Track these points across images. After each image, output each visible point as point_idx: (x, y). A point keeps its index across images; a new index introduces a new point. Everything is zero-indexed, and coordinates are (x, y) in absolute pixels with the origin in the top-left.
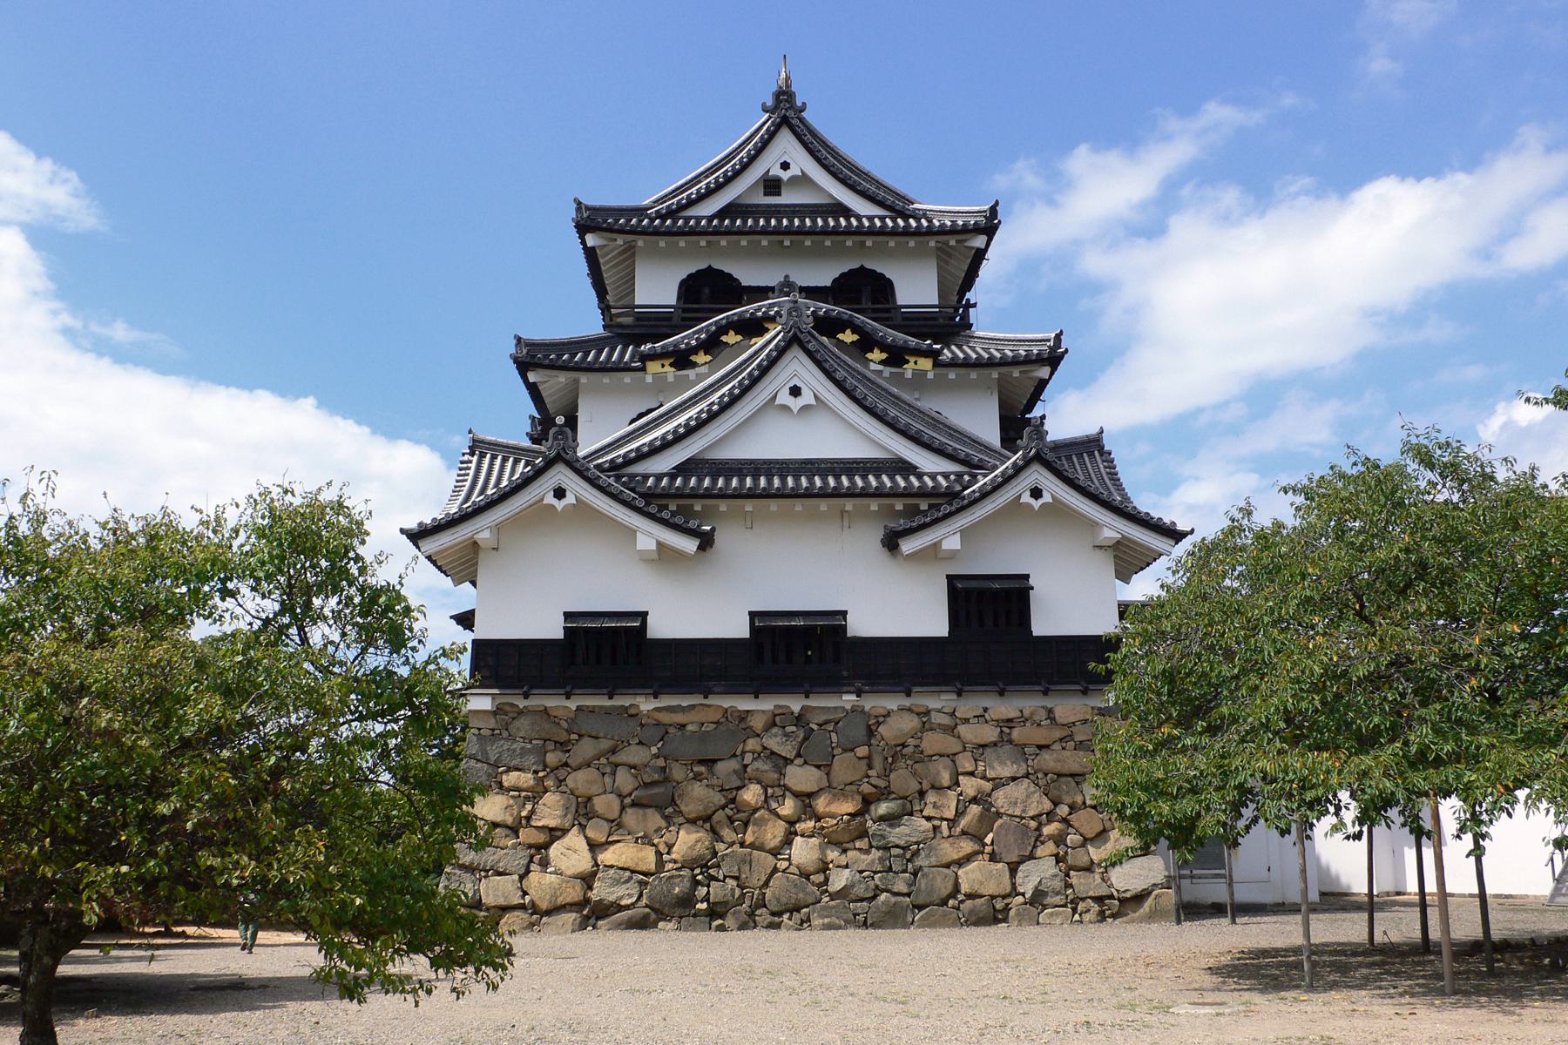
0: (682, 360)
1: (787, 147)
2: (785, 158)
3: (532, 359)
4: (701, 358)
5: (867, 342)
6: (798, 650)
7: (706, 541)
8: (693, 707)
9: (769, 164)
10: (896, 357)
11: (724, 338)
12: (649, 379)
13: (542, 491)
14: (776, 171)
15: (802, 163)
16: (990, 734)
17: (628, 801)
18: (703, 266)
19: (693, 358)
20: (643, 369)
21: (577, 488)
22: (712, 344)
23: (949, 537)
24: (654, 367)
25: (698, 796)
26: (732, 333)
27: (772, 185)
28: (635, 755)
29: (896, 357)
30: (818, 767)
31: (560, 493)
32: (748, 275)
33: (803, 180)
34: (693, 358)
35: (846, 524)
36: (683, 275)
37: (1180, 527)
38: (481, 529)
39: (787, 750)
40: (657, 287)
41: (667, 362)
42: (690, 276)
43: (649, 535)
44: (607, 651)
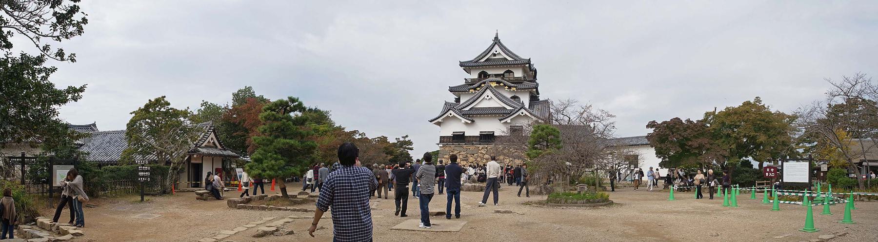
0: (475, 89)
1: (497, 48)
3: (452, 90)
5: (505, 85)
6: (487, 138)
7: (473, 121)
9: (493, 51)
10: (510, 87)
13: (448, 114)
15: (499, 50)
21: (453, 113)
22: (479, 86)
23: (508, 120)
25: (471, 159)
27: (495, 55)
29: (510, 87)
32: (489, 72)
33: (499, 54)
38: (440, 120)
40: (475, 75)
43: (464, 120)
44: (459, 138)
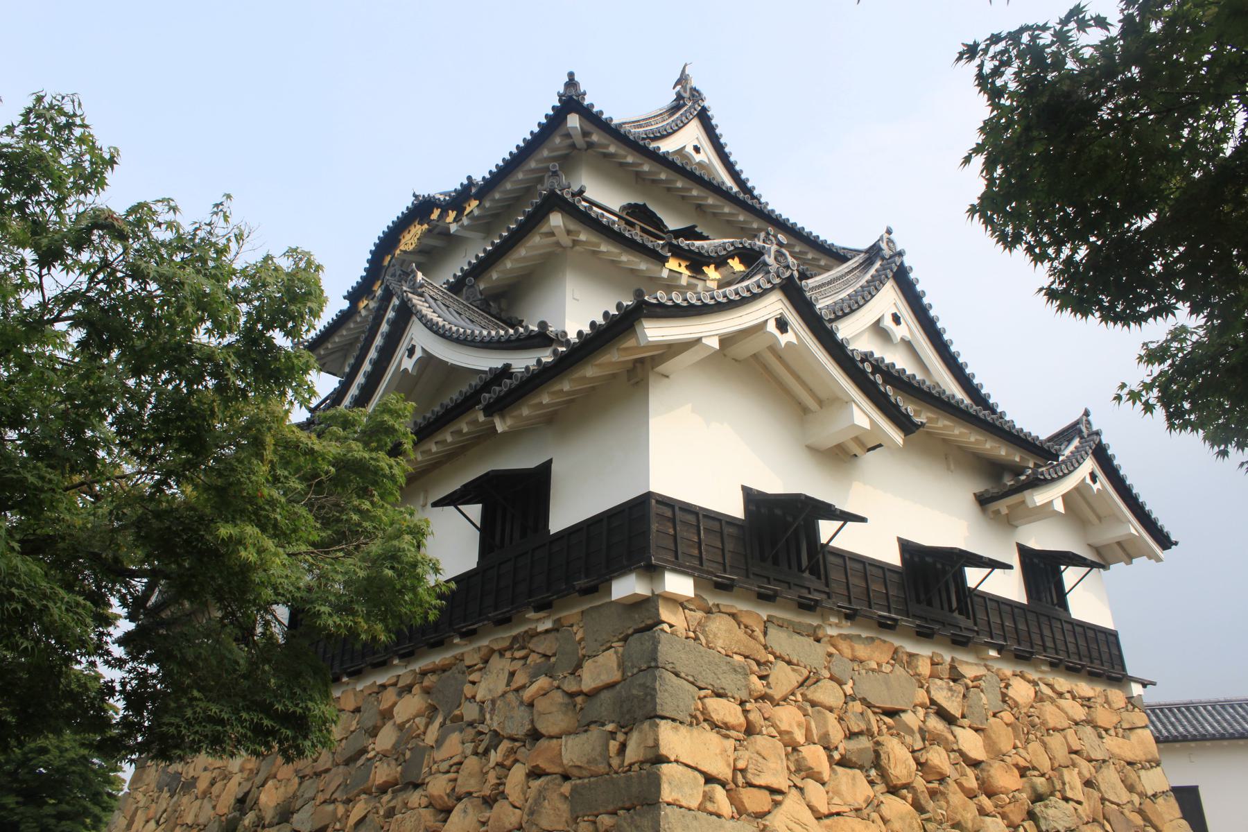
2: (696, 143)
4: (711, 271)
8: (872, 639)
11: (730, 261)
12: (665, 274)
14: (690, 150)
15: (707, 156)
16: (1079, 713)
17: (837, 756)
18: (641, 203)
19: (705, 269)
20: (663, 260)
22: (720, 262)
24: (673, 264)
26: (736, 259)
28: (828, 693)
30: (977, 730)
31: (782, 325)
34: (705, 269)
35: (952, 467)
36: (625, 203)
37: (1173, 539)
39: (954, 708)
41: (683, 264)
42: (630, 206)
